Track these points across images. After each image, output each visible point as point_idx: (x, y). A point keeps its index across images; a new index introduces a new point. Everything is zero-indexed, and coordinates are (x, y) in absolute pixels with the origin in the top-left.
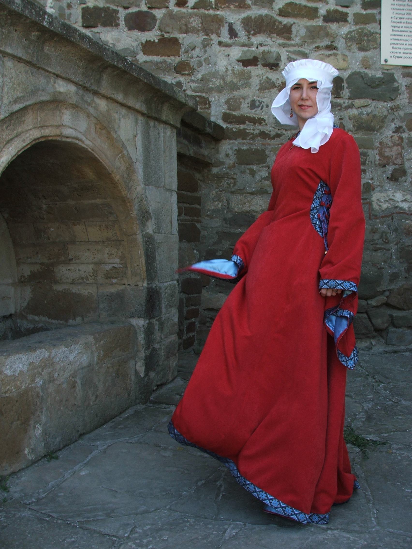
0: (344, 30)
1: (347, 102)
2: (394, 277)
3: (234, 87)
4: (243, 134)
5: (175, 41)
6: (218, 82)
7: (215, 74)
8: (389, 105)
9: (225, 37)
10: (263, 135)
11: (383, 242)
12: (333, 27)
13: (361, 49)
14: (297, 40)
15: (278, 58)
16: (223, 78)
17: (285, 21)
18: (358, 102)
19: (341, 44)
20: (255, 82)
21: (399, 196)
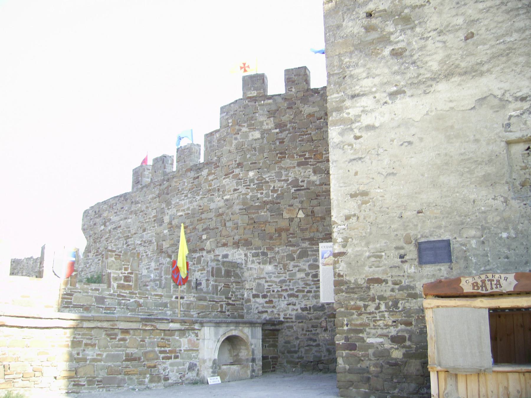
0: (312, 294)
1: (312, 312)
2: (325, 356)
3: (285, 311)
4: (287, 322)
5: (272, 301)
6: (282, 310)
7: (281, 308)
8: (323, 312)
9: (283, 299)
10: (292, 322)
11: (300, 346)
12: (309, 294)
13: (316, 299)
14: (300, 298)
15: (296, 303)
16: (283, 309)
17: (297, 294)
18: (315, 312)
19: (310, 298)
20: (290, 309)
21: (326, 336)
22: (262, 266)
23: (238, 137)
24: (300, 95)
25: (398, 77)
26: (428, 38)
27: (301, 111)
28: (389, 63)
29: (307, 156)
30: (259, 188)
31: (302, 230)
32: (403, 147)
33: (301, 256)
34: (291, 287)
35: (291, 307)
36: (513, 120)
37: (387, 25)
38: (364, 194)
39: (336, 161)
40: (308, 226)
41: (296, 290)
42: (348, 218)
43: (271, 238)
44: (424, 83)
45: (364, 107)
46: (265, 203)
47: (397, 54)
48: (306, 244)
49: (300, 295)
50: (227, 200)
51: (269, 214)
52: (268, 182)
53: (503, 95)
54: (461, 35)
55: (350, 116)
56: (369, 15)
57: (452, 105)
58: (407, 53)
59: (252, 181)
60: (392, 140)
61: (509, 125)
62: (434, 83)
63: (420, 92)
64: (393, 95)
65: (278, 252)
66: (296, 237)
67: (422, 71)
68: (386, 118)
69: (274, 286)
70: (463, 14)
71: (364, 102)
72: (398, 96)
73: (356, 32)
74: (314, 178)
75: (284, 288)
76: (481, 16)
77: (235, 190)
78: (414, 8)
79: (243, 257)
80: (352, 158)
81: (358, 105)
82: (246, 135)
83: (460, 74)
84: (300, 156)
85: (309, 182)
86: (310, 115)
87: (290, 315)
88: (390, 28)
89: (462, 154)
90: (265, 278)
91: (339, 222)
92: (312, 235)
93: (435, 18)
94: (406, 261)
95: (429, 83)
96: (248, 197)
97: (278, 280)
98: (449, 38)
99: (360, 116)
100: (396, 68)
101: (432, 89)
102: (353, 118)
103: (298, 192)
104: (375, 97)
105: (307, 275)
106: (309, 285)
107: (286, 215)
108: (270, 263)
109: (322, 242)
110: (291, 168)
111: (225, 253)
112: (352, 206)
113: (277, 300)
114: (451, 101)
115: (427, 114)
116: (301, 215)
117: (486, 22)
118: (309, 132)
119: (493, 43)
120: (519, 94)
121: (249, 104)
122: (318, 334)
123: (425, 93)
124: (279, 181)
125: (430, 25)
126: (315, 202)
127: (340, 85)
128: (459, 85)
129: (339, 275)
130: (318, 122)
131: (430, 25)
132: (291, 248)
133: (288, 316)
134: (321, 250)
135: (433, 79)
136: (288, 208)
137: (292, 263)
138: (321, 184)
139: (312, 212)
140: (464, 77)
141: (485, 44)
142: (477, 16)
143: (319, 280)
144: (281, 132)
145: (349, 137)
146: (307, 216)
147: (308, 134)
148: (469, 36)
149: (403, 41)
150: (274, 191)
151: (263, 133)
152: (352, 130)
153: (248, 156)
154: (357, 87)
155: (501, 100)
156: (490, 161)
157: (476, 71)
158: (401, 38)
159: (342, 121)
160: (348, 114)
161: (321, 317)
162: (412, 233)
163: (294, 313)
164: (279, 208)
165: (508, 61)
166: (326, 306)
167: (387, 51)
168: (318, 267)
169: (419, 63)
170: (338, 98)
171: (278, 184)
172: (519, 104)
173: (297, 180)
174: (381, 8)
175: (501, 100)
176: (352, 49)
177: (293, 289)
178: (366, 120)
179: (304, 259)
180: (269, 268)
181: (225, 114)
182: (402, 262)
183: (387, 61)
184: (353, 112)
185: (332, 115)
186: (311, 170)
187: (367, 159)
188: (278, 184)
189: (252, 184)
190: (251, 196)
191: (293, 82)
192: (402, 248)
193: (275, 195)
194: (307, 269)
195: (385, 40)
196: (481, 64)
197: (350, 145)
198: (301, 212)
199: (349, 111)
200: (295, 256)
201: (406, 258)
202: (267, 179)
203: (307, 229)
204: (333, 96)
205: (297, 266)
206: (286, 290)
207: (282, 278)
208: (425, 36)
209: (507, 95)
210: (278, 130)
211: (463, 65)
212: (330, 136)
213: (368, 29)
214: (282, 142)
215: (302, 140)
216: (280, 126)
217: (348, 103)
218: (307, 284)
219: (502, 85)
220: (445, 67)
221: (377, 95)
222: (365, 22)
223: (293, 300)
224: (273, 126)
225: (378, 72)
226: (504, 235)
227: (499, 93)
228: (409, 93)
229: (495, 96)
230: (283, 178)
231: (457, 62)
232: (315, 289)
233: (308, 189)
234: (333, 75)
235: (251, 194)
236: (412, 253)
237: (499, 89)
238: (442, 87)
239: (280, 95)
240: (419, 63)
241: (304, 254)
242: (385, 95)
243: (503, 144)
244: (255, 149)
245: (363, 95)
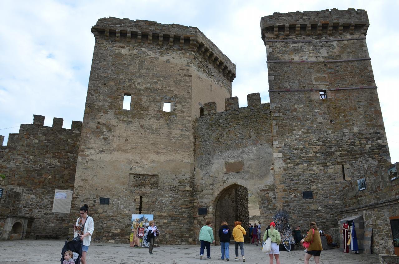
0: (49, 209)
2: (51, 232)
3: (37, 214)
4: (37, 218)
12: (48, 208)
22: (29, 195)
23: (28, 140)
24: (59, 130)
25: (104, 146)
26: (115, 137)
27: (57, 136)
28: (102, 141)
29: (57, 154)
30: (34, 163)
31: (50, 183)
32: (101, 168)
33: (47, 194)
34: (41, 205)
35: (40, 213)
36: (132, 168)
37: (104, 128)
38: (86, 180)
39: (79, 168)
40: (52, 182)
41: (43, 206)
42: (79, 187)
43: (36, 184)
44: (111, 150)
45: (91, 152)
46: (36, 170)
47: (105, 139)
48: (50, 189)
49: (45, 208)
50: (17, 165)
51: (37, 175)
52: (38, 162)
53: (132, 160)
54: (124, 139)
55: (86, 154)
56: (99, 123)
57: (117, 159)
58: (108, 139)
59: (31, 160)
60: (98, 165)
61: (131, 169)
62: (114, 151)
63: (109, 153)
64: (101, 151)
65: (38, 191)
66: (46, 186)
67: (111, 147)
68: (98, 158)
69: (34, 204)
70: (126, 133)
71: (92, 151)
72: (102, 152)
73: (93, 127)
74: (58, 164)
75: (38, 205)
76: (131, 135)
77: (23, 162)
78: (113, 126)
79: (22, 190)
80: (84, 168)
81: (89, 151)
82: (32, 140)
83: (122, 151)
84: (54, 154)
85: (55, 165)
86: (61, 139)
87: (39, 216)
88: (104, 130)
89: (117, 174)
90: (30, 200)
91: (77, 187)
92: (53, 186)
93: (118, 131)
94: (96, 203)
95: (113, 151)
96: (28, 166)
97: (36, 201)
98: (121, 139)
99: (89, 155)
100: (103, 143)
101: (113, 153)
102: (87, 155)
103: (50, 168)
104: (95, 151)
105: (49, 201)
106: (49, 205)
107: (44, 176)
108: (34, 194)
109: (57, 189)
110: (49, 158)
111: (12, 187)
112: (81, 183)
113: (34, 209)
114: (118, 158)
115: (110, 160)
116: (50, 177)
117: (132, 138)
118: (59, 145)
119: (132, 144)
120: (136, 161)
121: (36, 127)
122: (49, 224)
123: (111, 153)
124: (43, 162)
125: (117, 133)
126: (56, 173)
127: (85, 143)
128: (121, 154)
129: (74, 204)
130: (63, 142)
131: (117, 133)
132: (44, 190)
133: (38, 216)
134: (56, 192)
135: (114, 150)
136: (45, 173)
137: (43, 196)
138: (60, 167)
139: (55, 177)
140: (122, 152)
141: (130, 144)
142: (129, 135)
143: (53, 203)
144: (47, 142)
145: (85, 161)
146: (52, 178)
147: (59, 146)
148: (126, 140)
149: (107, 135)
150: (40, 166)
151: (39, 141)
152: (86, 159)
153: (31, 149)
154: (90, 146)
155: (131, 161)
156: (124, 178)
157: (126, 151)
158: (107, 134)
159: (83, 155)
160: (86, 153)
161: (52, 217)
162: (99, 195)
163: (41, 215)
164: (41, 173)
165: (135, 151)
166: (54, 214)
167: (102, 137)
168: (54, 198)
169: (111, 144)
170: (83, 147)
171: (42, 163)
172: (135, 164)
173: (51, 163)
174: (103, 122)
175: (131, 161)
176: (91, 132)
177: (42, 206)
178: (91, 157)
179: (49, 195)
180: (33, 196)
181: (23, 128)
182: (95, 202)
183: (101, 140)
184: (87, 153)
185: (80, 152)
186: (57, 161)
187: (89, 170)
188: (42, 163)
189: (31, 161)
190: (30, 166)
191: (57, 123)
192: (95, 198)
193: (40, 168)
194: (49, 199)
195: (102, 133)
196: (128, 149)
197: (84, 164)
198: (50, 176)
199: (86, 153)
200: (45, 193)
201: (97, 201)
202: (38, 160)
203: (51, 183)
204: (81, 146)
205: (45, 197)
206: (39, 206)
207: (38, 201)
208: (114, 136)
209: (133, 160)
210: (46, 142)
211: (123, 148)
212: (78, 159)
213: (98, 128)
214: (47, 147)
215: (56, 148)
216: (48, 140)
217: (86, 150)
218: (48, 204)
219: (132, 157)
220: (118, 147)
221: (96, 150)
222: (97, 125)
223: (41, 210)
224: (44, 139)
225: (98, 143)
226: (124, 199)
227: (131, 159)
228: (106, 152)
229: (130, 160)
230: (45, 161)
231: (122, 147)
232: (51, 207)
233: (55, 168)
234: (83, 139)
235: (30, 165)
236: (98, 200)
237: (131, 158)
238: (115, 153)
239: (50, 127)
240: (111, 144)
241: (48, 193)
242: (99, 151)
243: (129, 174)
244: (35, 147)
245: (92, 149)
